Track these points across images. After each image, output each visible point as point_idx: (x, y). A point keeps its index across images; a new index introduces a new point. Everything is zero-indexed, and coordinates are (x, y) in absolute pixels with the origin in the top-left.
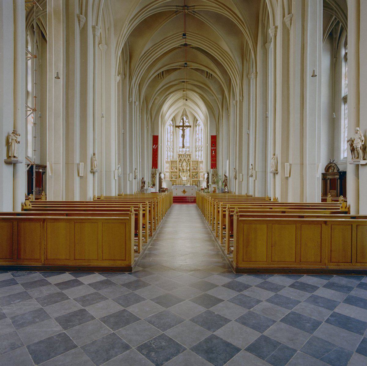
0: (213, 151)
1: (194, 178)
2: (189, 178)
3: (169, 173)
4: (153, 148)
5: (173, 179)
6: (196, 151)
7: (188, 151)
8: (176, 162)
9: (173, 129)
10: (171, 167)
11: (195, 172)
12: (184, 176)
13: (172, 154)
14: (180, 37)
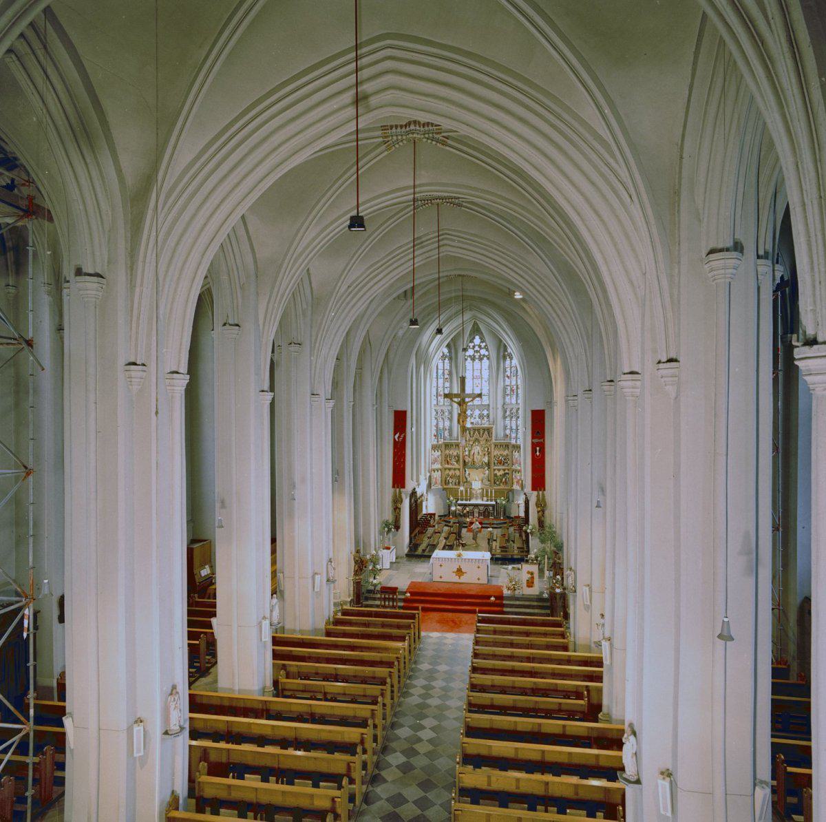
0: (538, 448)
2: (488, 483)
3: (440, 471)
4: (394, 439)
5: (450, 486)
9: (451, 367)
14: (432, 243)
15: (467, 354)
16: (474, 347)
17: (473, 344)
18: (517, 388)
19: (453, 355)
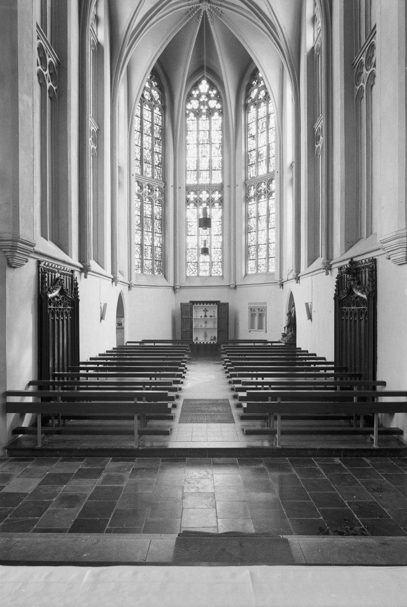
6: (247, 199)
7: (216, 199)
9: (164, 121)
13: (157, 210)
15: (189, 106)
16: (199, 96)
17: (197, 92)
19: (167, 103)
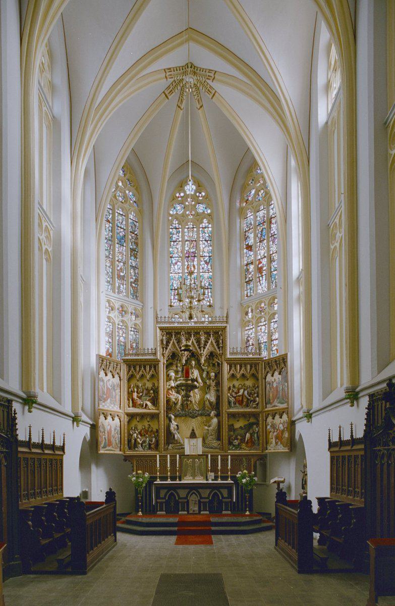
1: (238, 447)
2: (215, 443)
3: (117, 419)
5: (140, 451)
8: (154, 364)
10: (130, 394)
11: (244, 415)
12: (193, 435)
18: (271, 260)
